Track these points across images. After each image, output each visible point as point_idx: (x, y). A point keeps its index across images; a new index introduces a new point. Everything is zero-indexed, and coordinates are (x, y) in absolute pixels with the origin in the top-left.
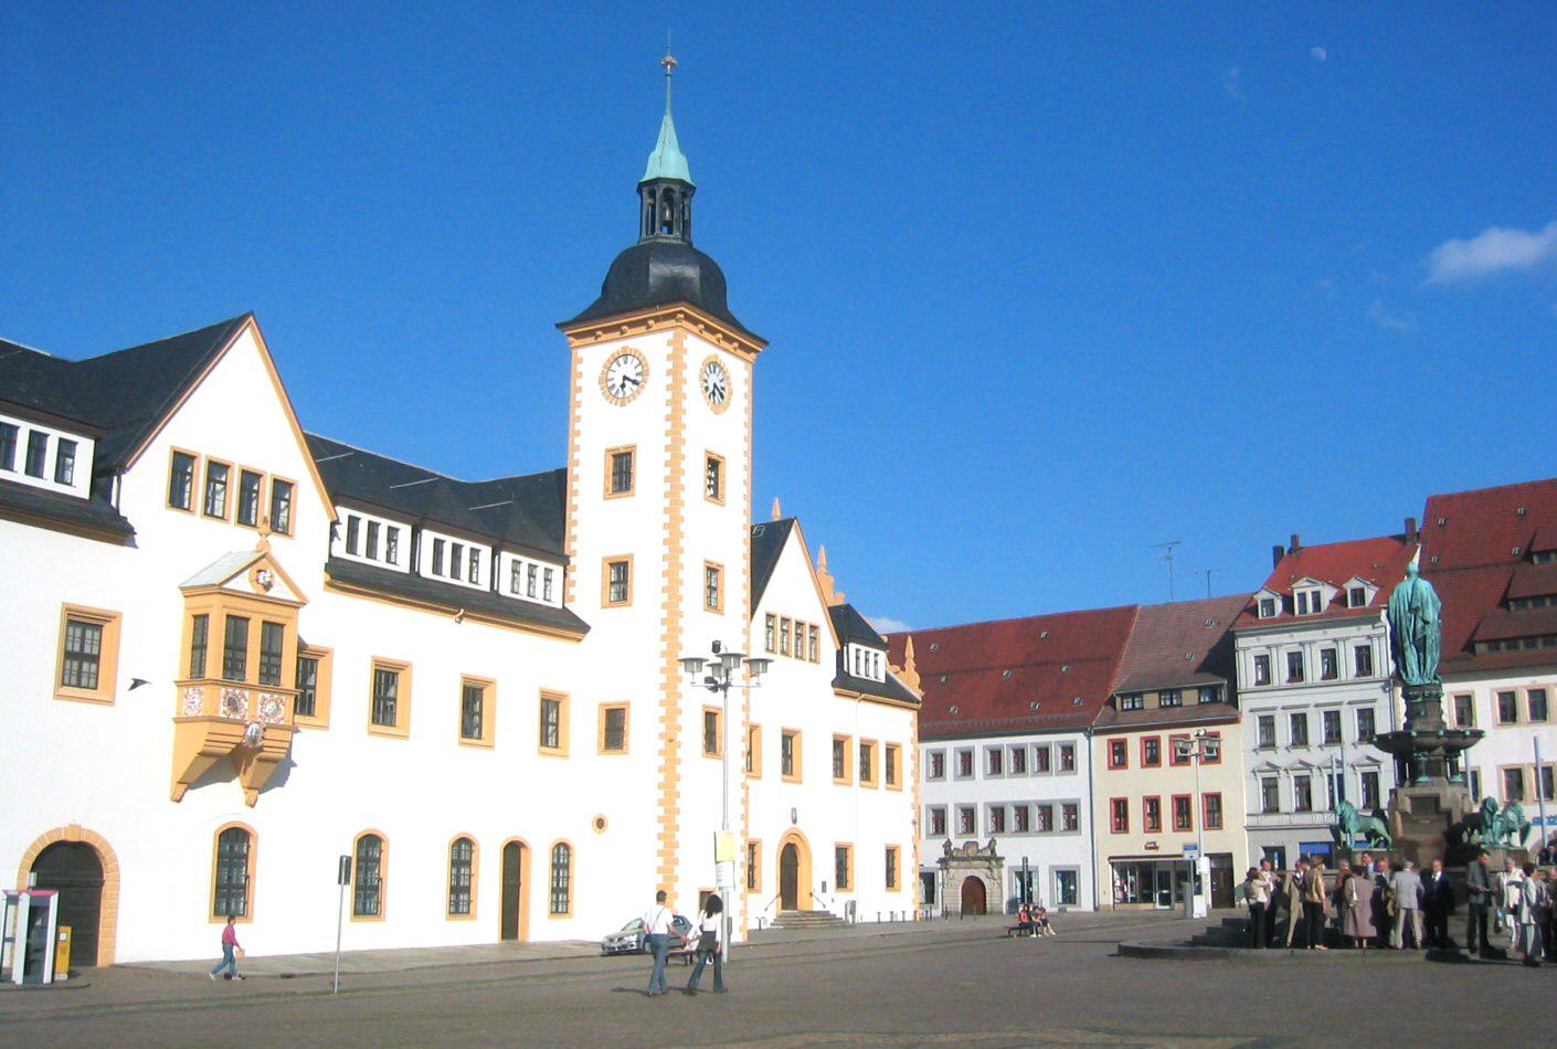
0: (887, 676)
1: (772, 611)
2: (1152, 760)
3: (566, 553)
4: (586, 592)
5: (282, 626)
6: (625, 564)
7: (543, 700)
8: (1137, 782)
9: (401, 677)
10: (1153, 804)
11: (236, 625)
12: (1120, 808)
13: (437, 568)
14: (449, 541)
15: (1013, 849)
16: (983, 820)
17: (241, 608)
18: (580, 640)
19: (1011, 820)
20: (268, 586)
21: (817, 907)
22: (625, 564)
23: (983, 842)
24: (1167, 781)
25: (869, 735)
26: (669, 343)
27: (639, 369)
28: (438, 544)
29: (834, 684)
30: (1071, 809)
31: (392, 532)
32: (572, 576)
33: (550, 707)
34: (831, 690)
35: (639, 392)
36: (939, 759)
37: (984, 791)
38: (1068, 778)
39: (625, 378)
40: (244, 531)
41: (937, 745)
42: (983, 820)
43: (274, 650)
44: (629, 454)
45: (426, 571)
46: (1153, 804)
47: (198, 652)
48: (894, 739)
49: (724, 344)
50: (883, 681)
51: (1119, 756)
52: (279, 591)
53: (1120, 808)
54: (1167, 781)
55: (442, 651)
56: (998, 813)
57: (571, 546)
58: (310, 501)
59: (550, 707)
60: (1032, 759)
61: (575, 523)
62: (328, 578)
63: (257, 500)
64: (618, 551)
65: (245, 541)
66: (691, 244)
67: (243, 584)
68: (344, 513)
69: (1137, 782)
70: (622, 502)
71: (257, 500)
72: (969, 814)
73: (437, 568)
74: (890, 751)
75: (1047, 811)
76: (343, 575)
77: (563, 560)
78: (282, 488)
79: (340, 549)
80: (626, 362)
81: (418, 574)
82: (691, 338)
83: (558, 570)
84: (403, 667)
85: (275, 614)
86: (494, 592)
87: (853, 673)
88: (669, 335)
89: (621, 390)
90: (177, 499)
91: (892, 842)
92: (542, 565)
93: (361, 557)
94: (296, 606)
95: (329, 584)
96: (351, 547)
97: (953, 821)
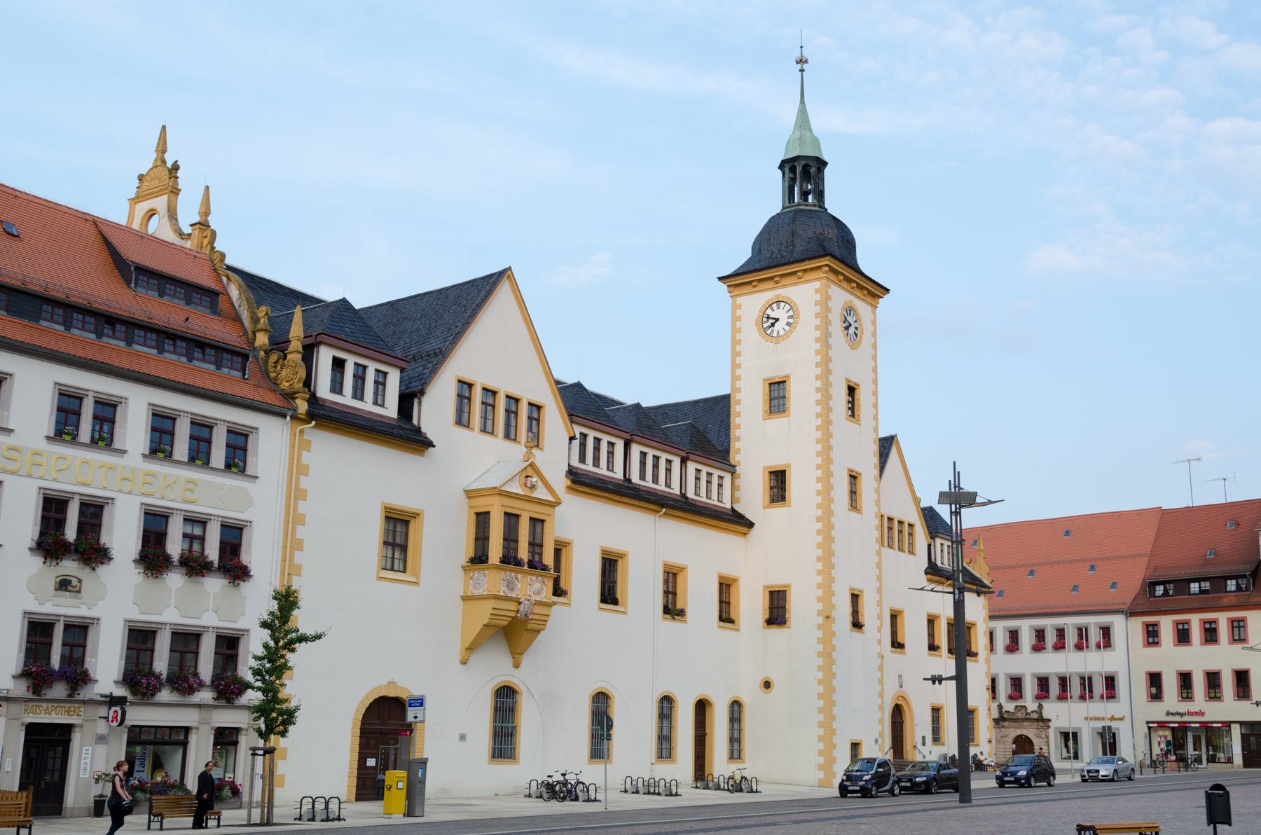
2: (1183, 637)
4: (751, 495)
5: (543, 521)
8: (1170, 658)
9: (620, 563)
10: (1185, 679)
11: (511, 519)
12: (1155, 680)
13: (642, 476)
14: (651, 453)
15: (1061, 714)
16: (1030, 688)
17: (515, 507)
19: (1054, 688)
21: (919, 758)
24: (1199, 658)
26: (817, 291)
27: (791, 313)
30: (1110, 681)
32: (737, 482)
35: (791, 332)
38: (1106, 654)
39: (777, 320)
42: (1030, 688)
43: (538, 541)
45: (635, 478)
49: (857, 292)
51: (1152, 635)
52: (541, 493)
53: (1155, 680)
54: (1199, 658)
55: (649, 542)
56: (1043, 682)
57: (735, 458)
64: (777, 463)
69: (1170, 658)
70: (778, 422)
72: (1017, 683)
73: (642, 476)
77: (732, 469)
81: (629, 481)
82: (833, 286)
83: (727, 478)
85: (539, 512)
86: (684, 495)
88: (817, 284)
92: (716, 473)
95: (568, 487)
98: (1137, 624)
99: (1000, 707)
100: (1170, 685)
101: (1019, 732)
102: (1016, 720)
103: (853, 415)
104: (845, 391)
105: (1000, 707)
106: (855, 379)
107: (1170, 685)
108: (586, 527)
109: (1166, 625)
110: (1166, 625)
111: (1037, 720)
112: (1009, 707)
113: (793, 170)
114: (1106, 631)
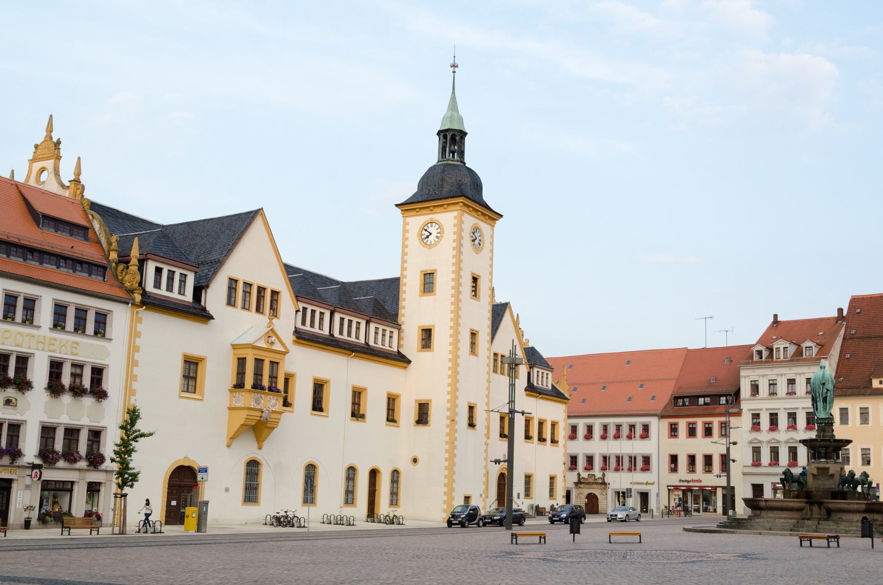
0: (553, 386)
1: (496, 352)
2: (692, 432)
3: (399, 323)
4: (411, 346)
6: (430, 330)
7: (389, 399)
8: (684, 446)
10: (692, 459)
12: (674, 459)
13: (341, 333)
14: (347, 318)
16: (598, 463)
19: (613, 463)
20: (272, 343)
22: (430, 330)
24: (701, 446)
25: (543, 417)
27: (439, 230)
28: (342, 319)
29: (526, 390)
30: (647, 460)
31: (322, 313)
32: (402, 335)
33: (392, 401)
34: (524, 393)
36: (574, 429)
37: (598, 447)
38: (645, 442)
40: (258, 316)
41: (574, 421)
42: (598, 463)
45: (336, 334)
46: (692, 459)
47: (240, 376)
48: (555, 419)
49: (482, 218)
50: (550, 388)
51: (673, 431)
53: (674, 459)
54: (701, 446)
55: (342, 373)
57: (401, 319)
58: (287, 302)
59: (392, 401)
60: (625, 431)
61: (404, 308)
62: (295, 338)
63: (263, 300)
64: (426, 324)
65: (262, 320)
67: (262, 344)
68: (301, 305)
69: (684, 446)
70: (428, 299)
71: (263, 300)
72: (590, 459)
73: (341, 333)
74: (554, 425)
75: (633, 460)
76: (301, 337)
77: (399, 327)
78: (275, 294)
79: (299, 326)
81: (333, 336)
82: (465, 215)
84: (327, 382)
86: (367, 344)
87: (535, 384)
88: (455, 214)
90: (231, 302)
91: (553, 473)
92: (388, 329)
93: (308, 328)
94: (284, 353)
96: (304, 322)
97: (581, 463)
98: (665, 424)
99: (579, 475)
100: (683, 462)
101: (590, 491)
102: (588, 483)
103: (475, 295)
104: (470, 280)
105: (579, 475)
106: (477, 272)
107: (683, 462)
109: (682, 425)
110: (682, 425)
111: (601, 484)
112: (584, 475)
114: (646, 428)
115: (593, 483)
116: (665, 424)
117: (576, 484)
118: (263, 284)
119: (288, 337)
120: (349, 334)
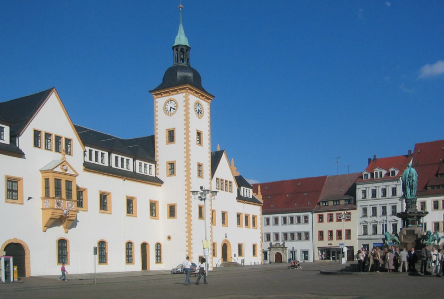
0: (253, 196)
1: (218, 177)
2: (331, 220)
3: (156, 160)
4: (162, 172)
5: (71, 182)
6: (173, 164)
7: (151, 203)
8: (326, 226)
10: (331, 233)
11: (58, 182)
12: (321, 234)
13: (117, 165)
14: (120, 157)
15: (290, 245)
16: (281, 237)
17: (59, 176)
18: (161, 186)
19: (289, 237)
20: (66, 170)
22: (173, 164)
23: (281, 243)
24: (335, 226)
25: (248, 213)
26: (184, 97)
27: (175, 105)
28: (117, 158)
29: (237, 198)
30: (307, 234)
31: (102, 154)
32: (157, 167)
33: (153, 206)
34: (236, 200)
35: (175, 112)
36: (268, 220)
37: (281, 229)
39: (171, 108)
40: (58, 154)
42: (281, 237)
44: (173, 131)
45: (113, 165)
46: (331, 233)
48: (255, 214)
49: (201, 97)
50: (251, 197)
51: (321, 219)
52: (70, 171)
53: (321, 234)
54: (335, 226)
55: (119, 189)
56: (286, 235)
57: (157, 158)
58: (77, 145)
60: (295, 220)
62: (84, 168)
63: (60, 144)
64: (171, 160)
65: (58, 157)
66: (190, 66)
67: (59, 169)
68: (87, 149)
69: (326, 226)
70: (171, 145)
71: (60, 144)
72: (277, 235)
73: (117, 165)
74: (254, 217)
75: (300, 234)
76: (88, 167)
77: (155, 163)
78: (68, 141)
79: (87, 159)
80: (171, 103)
81: (111, 167)
83: (153, 166)
84: (109, 193)
85: (69, 178)
86: (134, 172)
87: (242, 195)
88: (184, 94)
89: (170, 112)
90: (36, 144)
91: (255, 243)
92: (148, 164)
93: (93, 161)
95: (84, 170)
96: (90, 158)
97: (272, 237)
99: (271, 244)
100: (326, 235)
101: (277, 251)
102: (275, 248)
103: (200, 143)
104: (196, 134)
105: (271, 244)
106: (200, 130)
107: (326, 235)
108: (93, 184)
111: (282, 248)
112: (274, 243)
113: (177, 50)
115: (279, 248)
116: (316, 216)
117: (269, 248)
118: (59, 134)
119: (79, 168)
120: (122, 166)
